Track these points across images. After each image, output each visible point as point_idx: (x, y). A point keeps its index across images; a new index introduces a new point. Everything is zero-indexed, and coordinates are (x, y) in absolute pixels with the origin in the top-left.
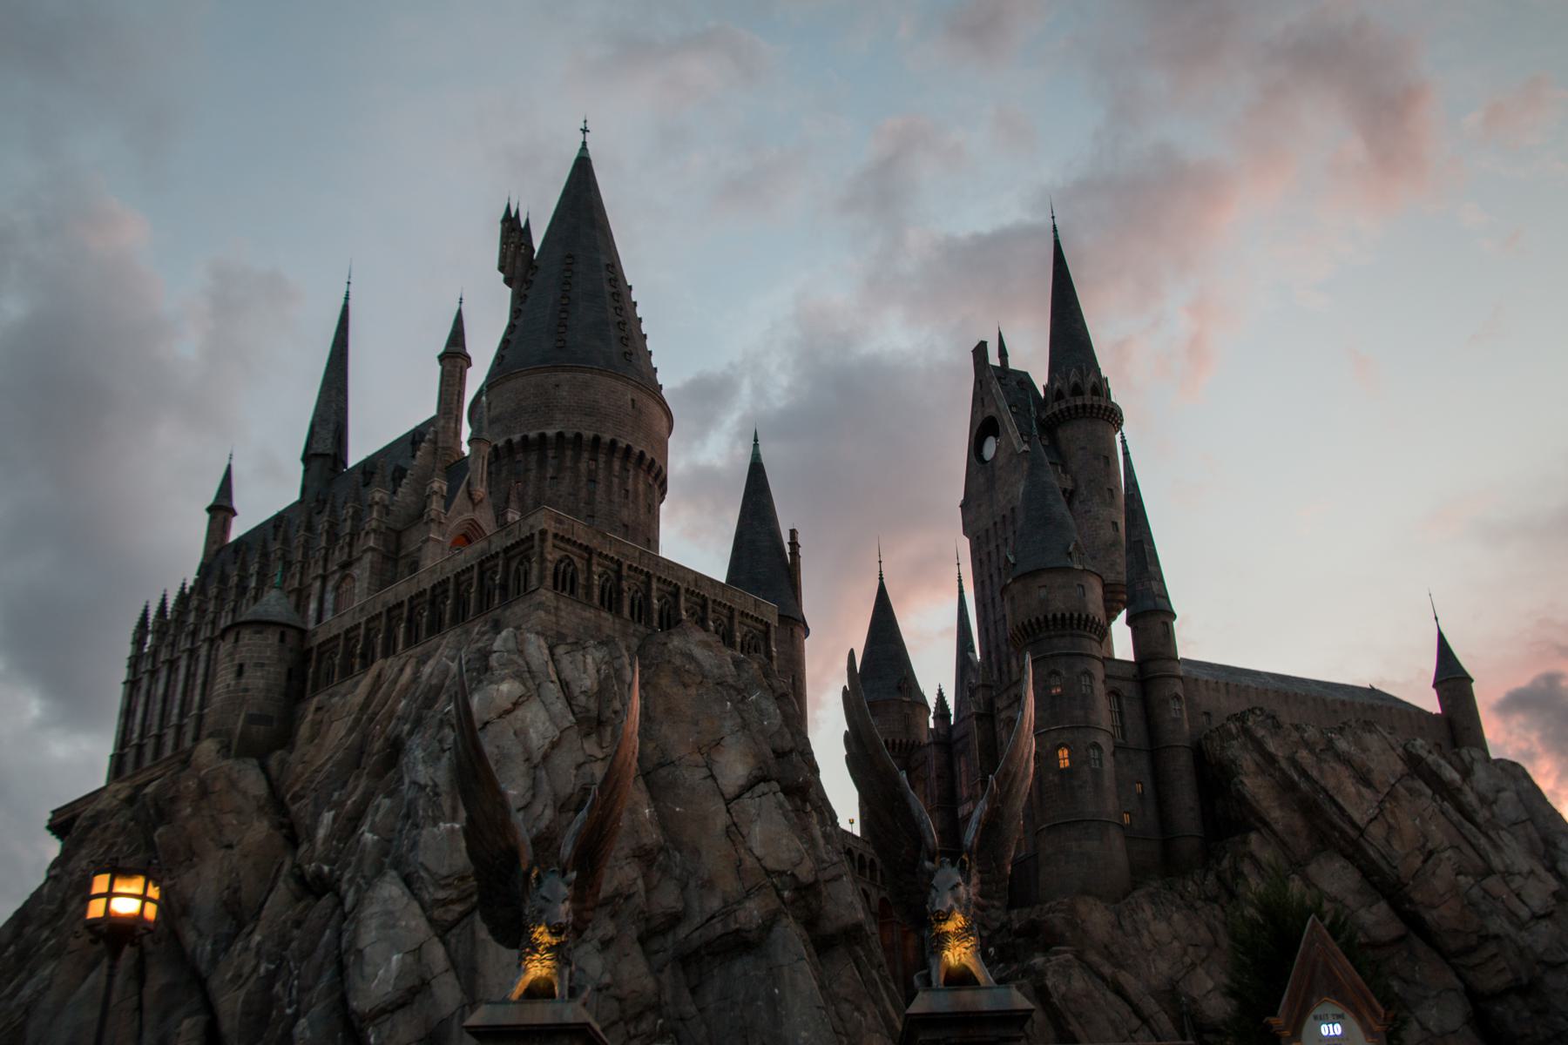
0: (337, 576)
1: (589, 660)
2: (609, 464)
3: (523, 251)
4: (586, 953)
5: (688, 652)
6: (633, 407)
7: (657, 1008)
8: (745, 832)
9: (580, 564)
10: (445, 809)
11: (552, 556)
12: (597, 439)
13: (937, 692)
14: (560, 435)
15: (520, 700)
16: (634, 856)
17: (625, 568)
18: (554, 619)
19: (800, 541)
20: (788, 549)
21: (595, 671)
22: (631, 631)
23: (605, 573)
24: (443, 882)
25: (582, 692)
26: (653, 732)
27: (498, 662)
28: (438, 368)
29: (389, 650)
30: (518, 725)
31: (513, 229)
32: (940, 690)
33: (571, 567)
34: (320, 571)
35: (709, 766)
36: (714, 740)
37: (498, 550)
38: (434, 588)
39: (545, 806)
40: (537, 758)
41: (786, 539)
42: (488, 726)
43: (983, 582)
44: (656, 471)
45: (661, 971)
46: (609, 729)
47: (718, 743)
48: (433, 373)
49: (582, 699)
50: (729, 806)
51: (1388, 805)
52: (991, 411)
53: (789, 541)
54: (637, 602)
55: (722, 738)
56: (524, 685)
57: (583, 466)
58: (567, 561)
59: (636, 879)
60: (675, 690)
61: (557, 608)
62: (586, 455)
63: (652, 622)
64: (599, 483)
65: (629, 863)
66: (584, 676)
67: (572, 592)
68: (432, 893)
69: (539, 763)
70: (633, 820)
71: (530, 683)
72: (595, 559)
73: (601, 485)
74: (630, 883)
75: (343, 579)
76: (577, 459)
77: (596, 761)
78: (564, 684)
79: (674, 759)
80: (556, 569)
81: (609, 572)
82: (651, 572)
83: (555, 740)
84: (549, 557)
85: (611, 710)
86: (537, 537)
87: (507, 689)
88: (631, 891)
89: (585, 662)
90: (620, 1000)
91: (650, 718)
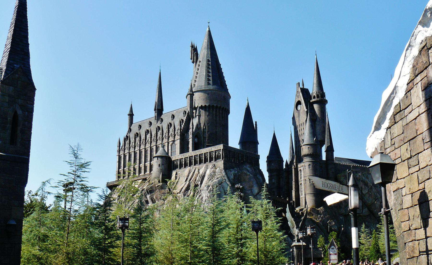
17: (235, 153)
20: (255, 126)
35: (251, 190)
38: (200, 155)
41: (254, 124)
43: (296, 137)
47: (253, 186)
51: (370, 190)
52: (299, 99)
62: (215, 110)
75: (173, 144)
86: (221, 150)
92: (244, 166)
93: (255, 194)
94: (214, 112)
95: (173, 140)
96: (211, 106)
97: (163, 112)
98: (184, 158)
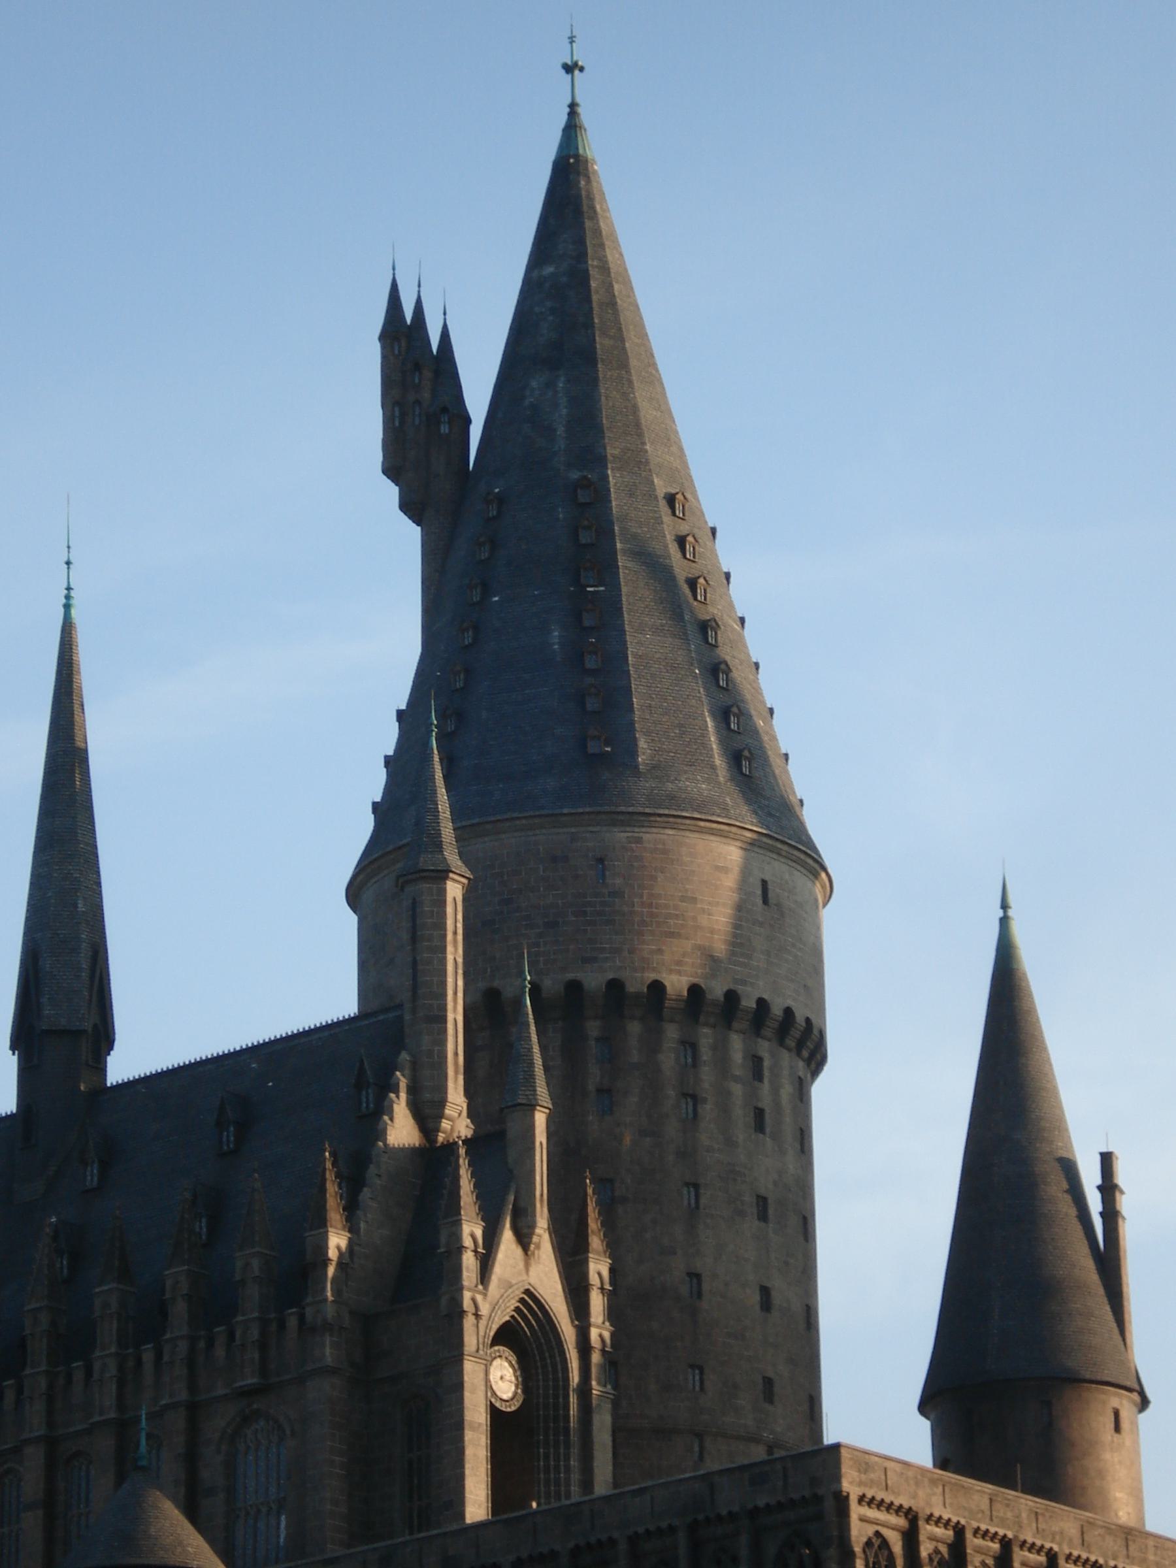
2: (721, 1049)
3: (444, 429)
6: (765, 901)
17: (969, 1535)
19: (1122, 1177)
37: (736, 1509)
41: (1090, 1178)
44: (797, 1034)
57: (668, 1061)
64: (705, 1100)
73: (708, 1107)
82: (1010, 1535)
95: (251, 1381)
96: (631, 988)
97: (111, 1060)
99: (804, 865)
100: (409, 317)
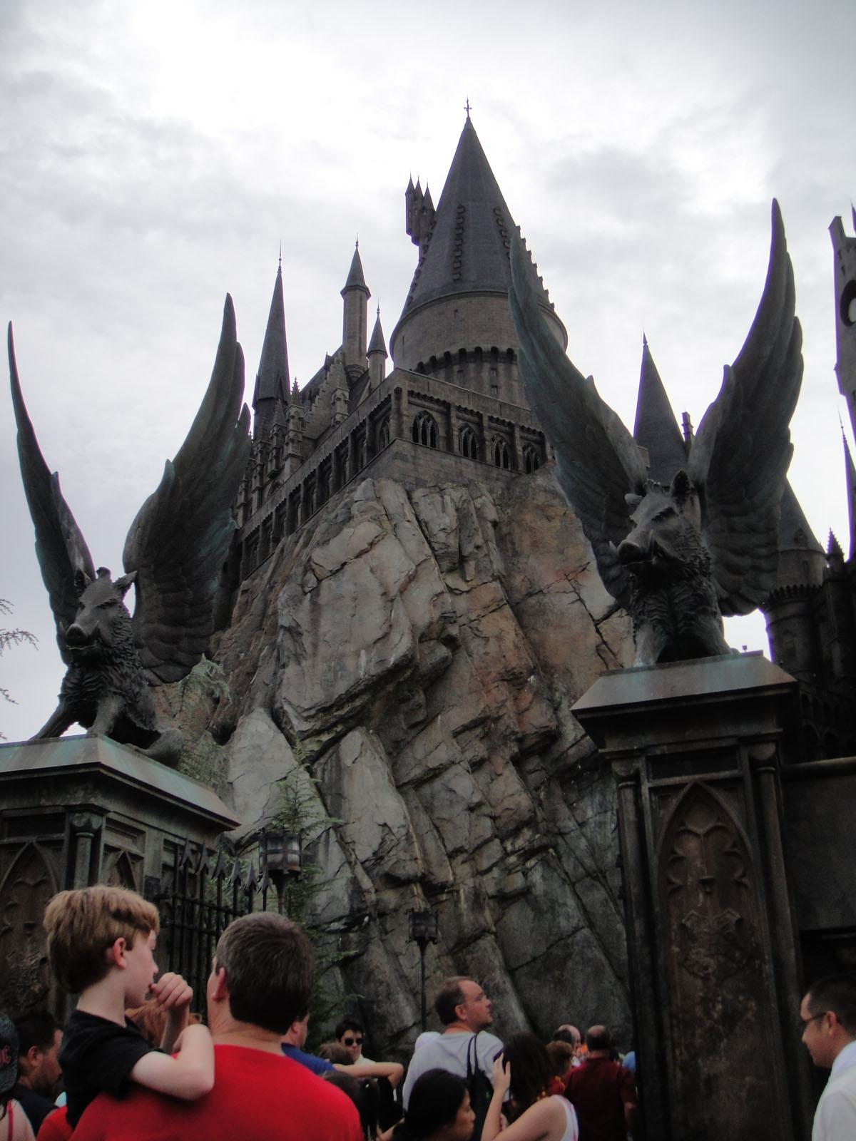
0: (269, 487)
1: (447, 498)
3: (425, 214)
4: (456, 775)
5: (552, 489)
7: (530, 823)
8: (615, 650)
9: (438, 418)
10: (305, 646)
11: (410, 412)
12: (495, 350)
13: (829, 535)
14: (462, 351)
15: (377, 539)
16: (503, 680)
17: (485, 419)
18: (412, 467)
21: (454, 510)
22: (495, 476)
23: (466, 426)
24: (305, 714)
25: (440, 530)
26: (520, 565)
27: (358, 511)
28: (342, 301)
29: (292, 529)
30: (374, 563)
31: (416, 198)
32: (831, 533)
33: (431, 422)
34: (258, 485)
36: (581, 566)
39: (403, 635)
40: (394, 591)
41: (680, 421)
42: (346, 566)
45: (537, 789)
46: (472, 563)
48: (337, 305)
49: (441, 537)
50: (598, 627)
53: (682, 423)
54: (501, 451)
55: (588, 563)
56: (381, 525)
57: (486, 375)
58: (426, 416)
59: (504, 701)
60: (539, 523)
61: (414, 457)
63: (518, 467)
64: (501, 388)
65: (497, 687)
66: (444, 514)
67: (433, 445)
68: (299, 725)
69: (396, 596)
70: (500, 646)
71: (387, 525)
72: (453, 413)
74: (500, 705)
76: (479, 371)
77: (460, 594)
78: (423, 524)
79: (542, 588)
80: (415, 424)
81: (470, 425)
82: (513, 422)
83: (410, 573)
84: (405, 412)
85: (472, 545)
87: (362, 531)
88: (501, 713)
89: (443, 501)
90: (494, 818)
91: (517, 552)
92: (535, 480)
93: (598, 612)
94: (486, 375)
98: (273, 510)
99: (551, 316)
100: (415, 187)
